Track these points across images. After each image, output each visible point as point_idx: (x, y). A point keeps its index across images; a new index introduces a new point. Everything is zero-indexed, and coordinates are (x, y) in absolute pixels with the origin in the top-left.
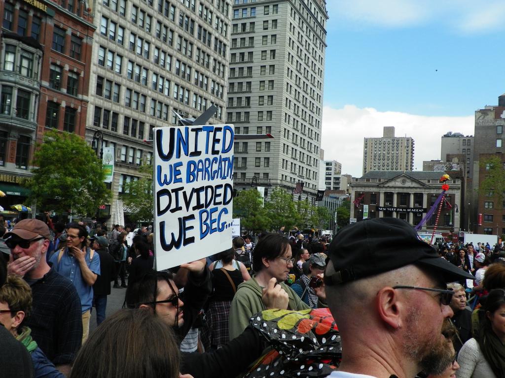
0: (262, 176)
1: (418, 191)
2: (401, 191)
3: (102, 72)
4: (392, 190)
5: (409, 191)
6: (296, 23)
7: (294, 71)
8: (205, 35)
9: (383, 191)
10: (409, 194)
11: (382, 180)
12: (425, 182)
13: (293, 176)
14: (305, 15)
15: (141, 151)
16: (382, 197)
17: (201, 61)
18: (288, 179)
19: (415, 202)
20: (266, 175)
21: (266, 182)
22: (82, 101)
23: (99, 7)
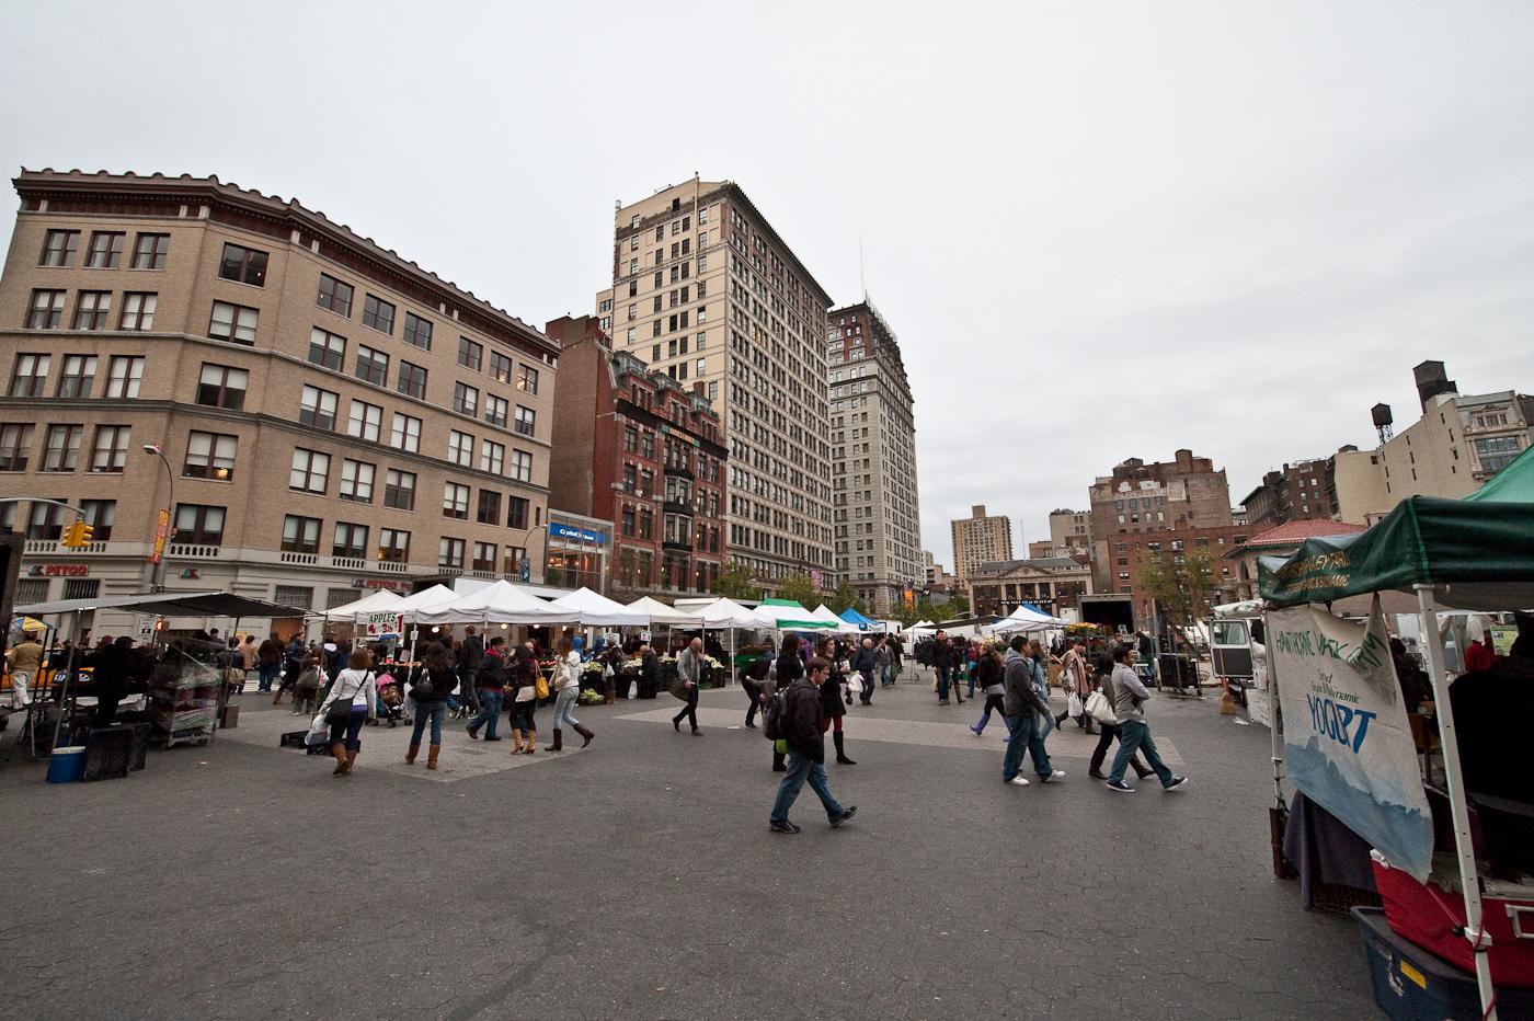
0: (866, 576)
1: (1044, 581)
2: (1024, 582)
3: (735, 491)
4: (1014, 582)
5: (1033, 581)
6: (885, 414)
7: (889, 463)
8: (811, 440)
9: (1004, 583)
10: (1034, 585)
11: (1001, 572)
12: (1050, 570)
13: (899, 574)
14: (893, 404)
15: (769, 563)
16: (1003, 590)
17: (778, 449)
18: (895, 578)
19: (1041, 592)
20: (871, 575)
21: (872, 583)
22: (722, 520)
23: (729, 431)
